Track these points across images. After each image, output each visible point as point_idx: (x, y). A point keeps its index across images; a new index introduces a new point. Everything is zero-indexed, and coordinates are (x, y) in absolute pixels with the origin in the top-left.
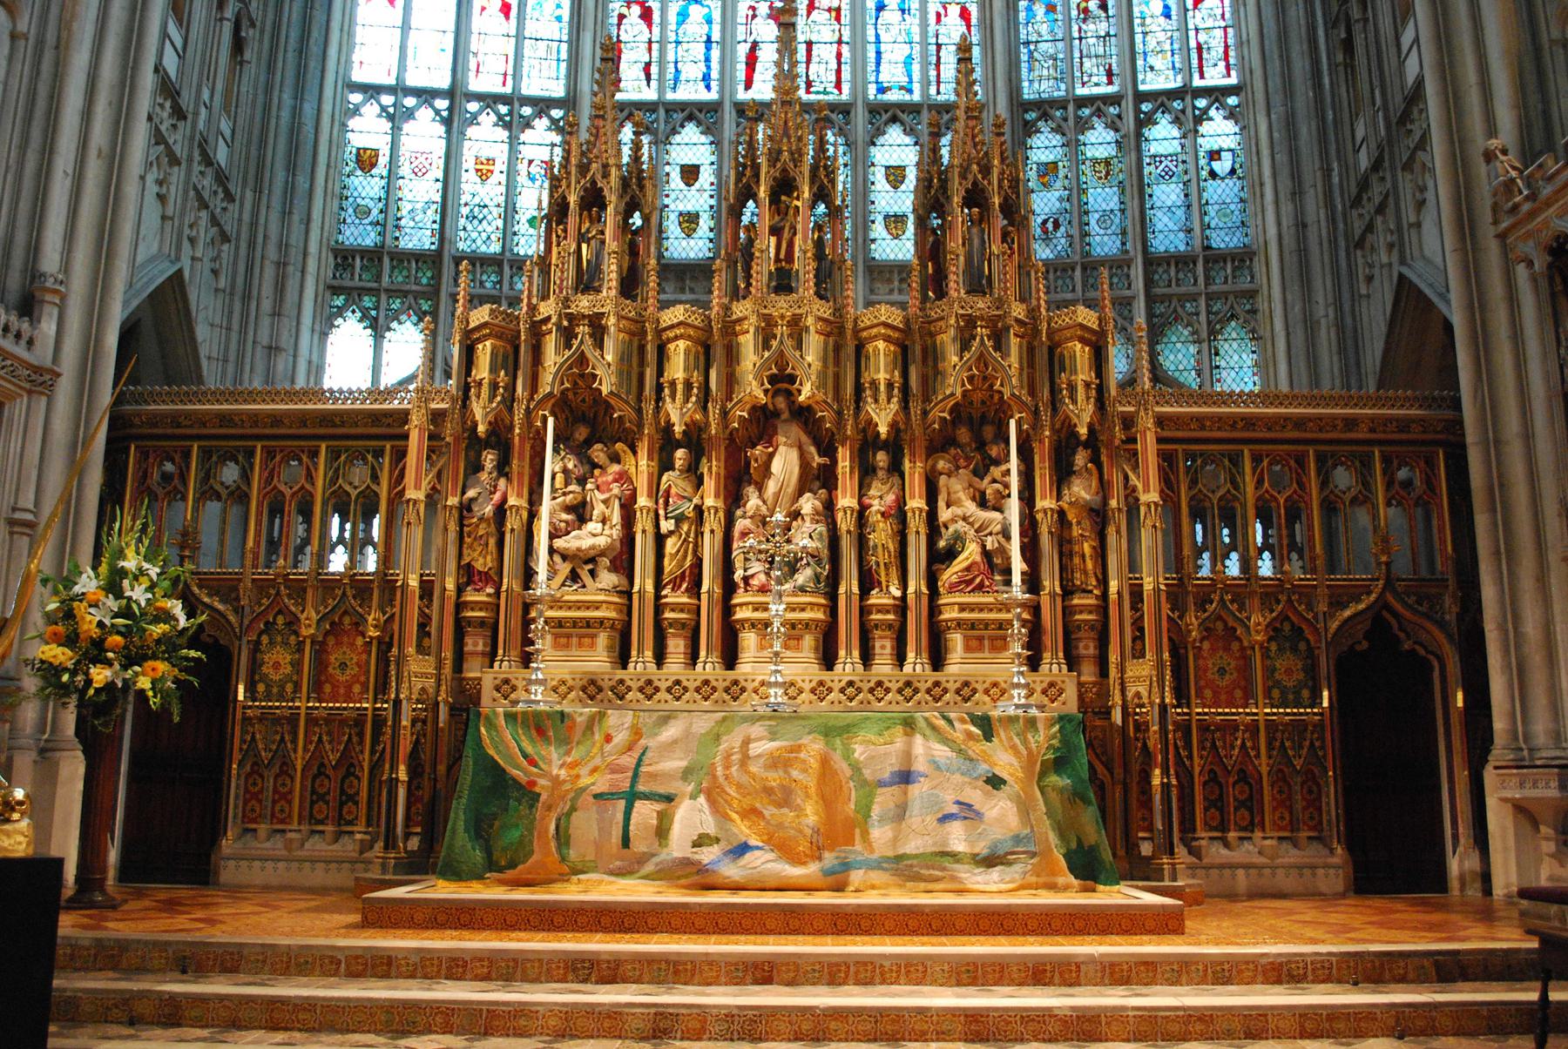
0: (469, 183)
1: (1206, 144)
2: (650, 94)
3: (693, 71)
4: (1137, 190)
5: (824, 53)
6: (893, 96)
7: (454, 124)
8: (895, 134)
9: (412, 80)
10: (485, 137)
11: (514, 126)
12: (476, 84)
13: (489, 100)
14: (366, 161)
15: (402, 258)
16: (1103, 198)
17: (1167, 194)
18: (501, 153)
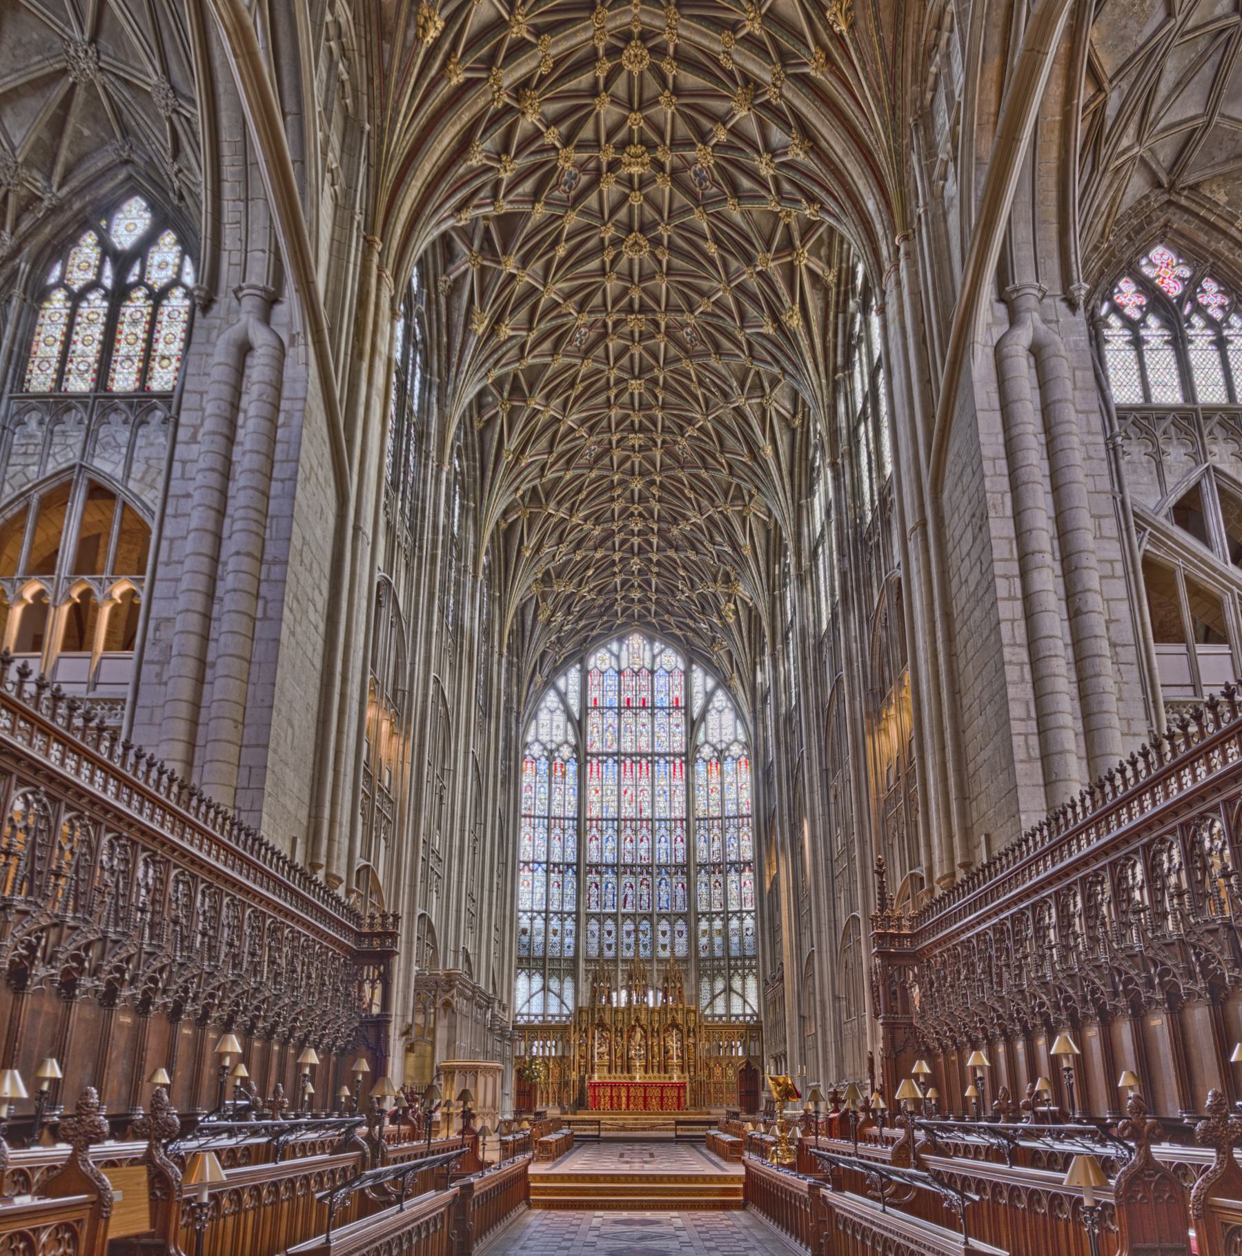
0: (551, 936)
1: (745, 926)
2: (598, 910)
3: (609, 903)
4: (726, 939)
5: (645, 898)
6: (663, 911)
7: (547, 920)
8: (664, 922)
9: (535, 908)
10: (555, 923)
11: (562, 920)
12: (551, 908)
13: (556, 913)
14: (524, 932)
15: (535, 959)
16: (718, 940)
17: (735, 940)
18: (559, 928)
